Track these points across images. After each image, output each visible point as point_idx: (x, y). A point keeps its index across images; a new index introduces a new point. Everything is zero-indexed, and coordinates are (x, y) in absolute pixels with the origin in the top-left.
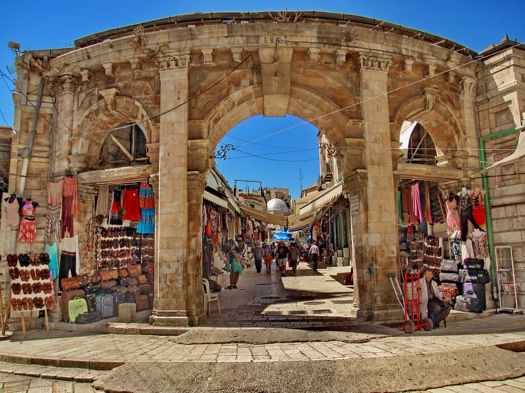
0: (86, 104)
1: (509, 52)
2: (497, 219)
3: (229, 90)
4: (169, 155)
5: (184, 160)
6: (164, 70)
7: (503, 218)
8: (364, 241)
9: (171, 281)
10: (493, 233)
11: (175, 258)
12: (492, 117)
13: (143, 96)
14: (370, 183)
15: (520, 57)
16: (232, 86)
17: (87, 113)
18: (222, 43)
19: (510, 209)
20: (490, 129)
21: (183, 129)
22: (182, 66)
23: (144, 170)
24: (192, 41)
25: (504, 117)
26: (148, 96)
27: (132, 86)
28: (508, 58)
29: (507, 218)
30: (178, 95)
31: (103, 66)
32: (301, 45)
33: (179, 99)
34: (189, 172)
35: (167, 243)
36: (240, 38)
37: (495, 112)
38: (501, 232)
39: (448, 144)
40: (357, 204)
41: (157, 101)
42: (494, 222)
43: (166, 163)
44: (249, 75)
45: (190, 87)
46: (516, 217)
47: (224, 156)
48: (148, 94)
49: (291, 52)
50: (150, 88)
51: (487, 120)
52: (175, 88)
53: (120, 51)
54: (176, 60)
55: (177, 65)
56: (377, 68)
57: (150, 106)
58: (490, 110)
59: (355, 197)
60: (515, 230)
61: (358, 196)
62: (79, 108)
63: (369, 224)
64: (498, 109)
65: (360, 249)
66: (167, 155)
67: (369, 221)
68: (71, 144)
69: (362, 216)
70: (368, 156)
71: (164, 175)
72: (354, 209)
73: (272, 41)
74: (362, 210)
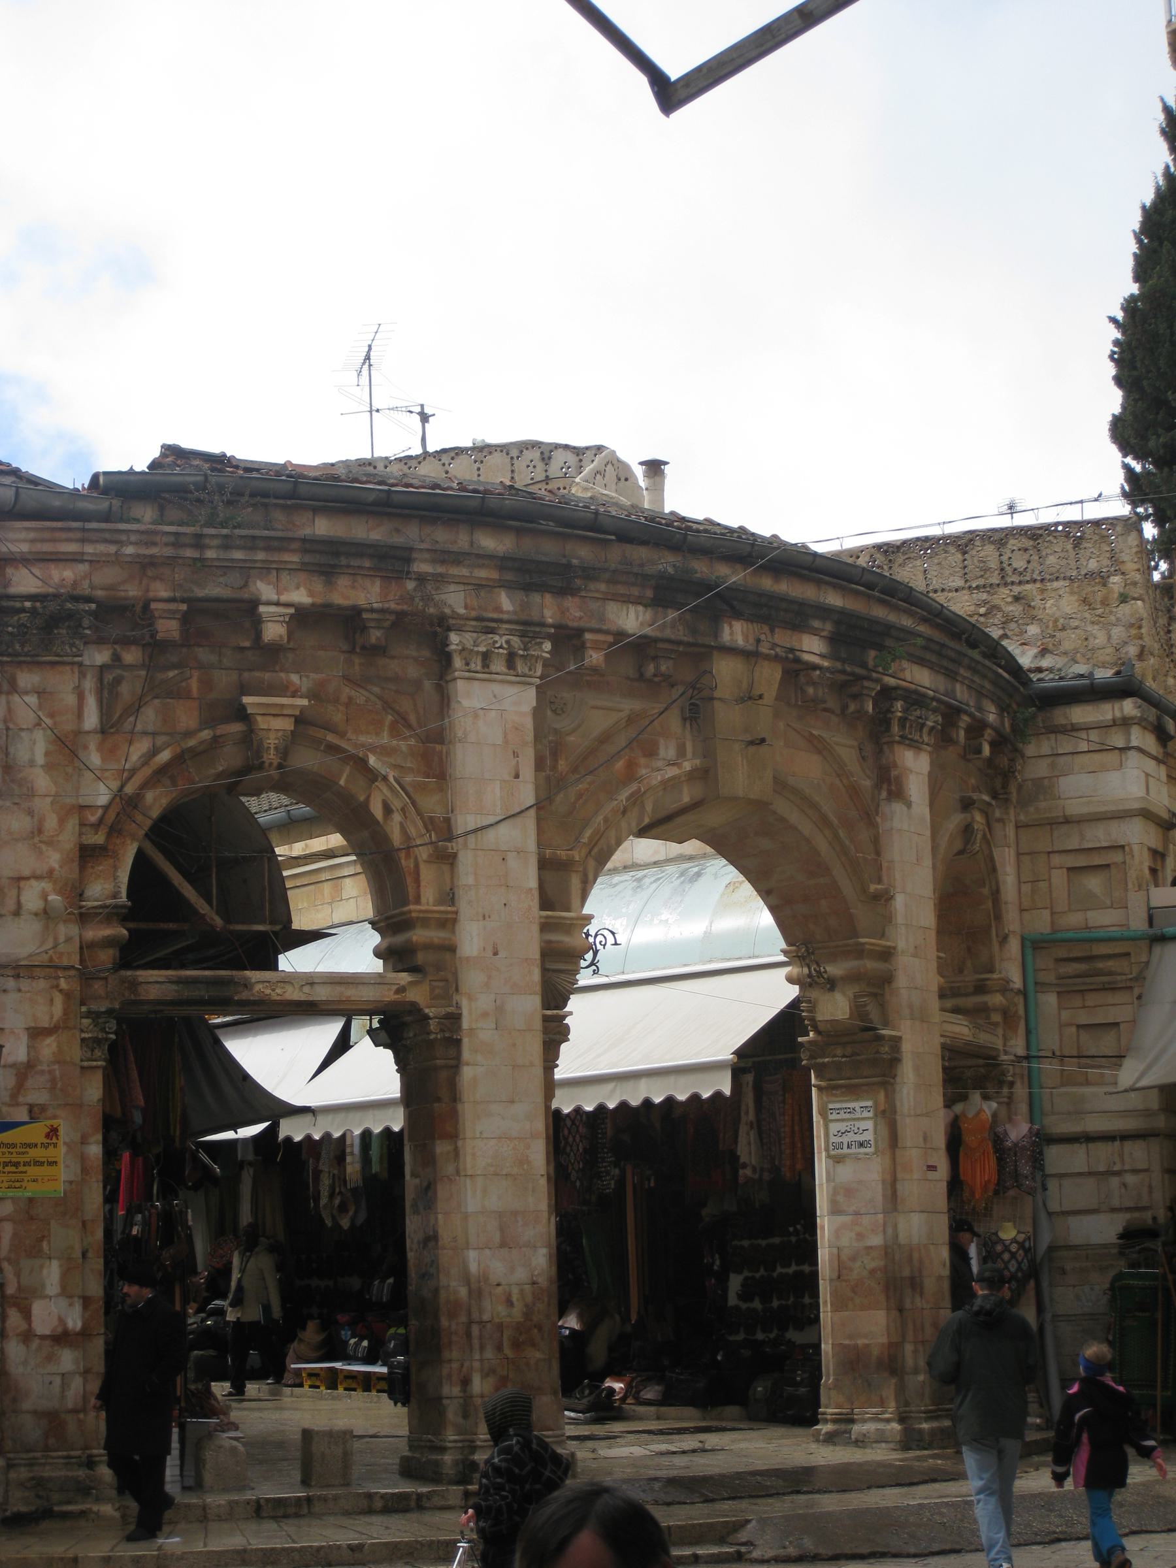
1: (1129, 707)
2: (1062, 1176)
4: (496, 954)
6: (469, 671)
7: (1080, 1174)
9: (516, 1345)
11: (521, 1274)
12: (1059, 878)
13: (385, 739)
14: (907, 1073)
20: (1052, 914)
21: (531, 881)
22: (526, 671)
23: (401, 990)
26: (403, 745)
27: (344, 698)
28: (1125, 723)
29: (1090, 1174)
30: (514, 762)
31: (262, 609)
33: (517, 776)
34: (549, 1012)
35: (502, 1229)
37: (1070, 865)
39: (969, 949)
40: (869, 1125)
43: (489, 977)
45: (537, 738)
46: (1118, 1173)
47: (592, 964)
49: (778, 675)
51: (1043, 885)
52: (506, 742)
53: (328, 573)
57: (409, 779)
58: (1056, 860)
59: (856, 1105)
60: (1113, 1210)
61: (869, 1103)
63: (899, 1186)
64: (1081, 861)
66: (489, 953)
67: (899, 1176)
70: (904, 992)
71: (485, 1015)
72: (845, 1139)
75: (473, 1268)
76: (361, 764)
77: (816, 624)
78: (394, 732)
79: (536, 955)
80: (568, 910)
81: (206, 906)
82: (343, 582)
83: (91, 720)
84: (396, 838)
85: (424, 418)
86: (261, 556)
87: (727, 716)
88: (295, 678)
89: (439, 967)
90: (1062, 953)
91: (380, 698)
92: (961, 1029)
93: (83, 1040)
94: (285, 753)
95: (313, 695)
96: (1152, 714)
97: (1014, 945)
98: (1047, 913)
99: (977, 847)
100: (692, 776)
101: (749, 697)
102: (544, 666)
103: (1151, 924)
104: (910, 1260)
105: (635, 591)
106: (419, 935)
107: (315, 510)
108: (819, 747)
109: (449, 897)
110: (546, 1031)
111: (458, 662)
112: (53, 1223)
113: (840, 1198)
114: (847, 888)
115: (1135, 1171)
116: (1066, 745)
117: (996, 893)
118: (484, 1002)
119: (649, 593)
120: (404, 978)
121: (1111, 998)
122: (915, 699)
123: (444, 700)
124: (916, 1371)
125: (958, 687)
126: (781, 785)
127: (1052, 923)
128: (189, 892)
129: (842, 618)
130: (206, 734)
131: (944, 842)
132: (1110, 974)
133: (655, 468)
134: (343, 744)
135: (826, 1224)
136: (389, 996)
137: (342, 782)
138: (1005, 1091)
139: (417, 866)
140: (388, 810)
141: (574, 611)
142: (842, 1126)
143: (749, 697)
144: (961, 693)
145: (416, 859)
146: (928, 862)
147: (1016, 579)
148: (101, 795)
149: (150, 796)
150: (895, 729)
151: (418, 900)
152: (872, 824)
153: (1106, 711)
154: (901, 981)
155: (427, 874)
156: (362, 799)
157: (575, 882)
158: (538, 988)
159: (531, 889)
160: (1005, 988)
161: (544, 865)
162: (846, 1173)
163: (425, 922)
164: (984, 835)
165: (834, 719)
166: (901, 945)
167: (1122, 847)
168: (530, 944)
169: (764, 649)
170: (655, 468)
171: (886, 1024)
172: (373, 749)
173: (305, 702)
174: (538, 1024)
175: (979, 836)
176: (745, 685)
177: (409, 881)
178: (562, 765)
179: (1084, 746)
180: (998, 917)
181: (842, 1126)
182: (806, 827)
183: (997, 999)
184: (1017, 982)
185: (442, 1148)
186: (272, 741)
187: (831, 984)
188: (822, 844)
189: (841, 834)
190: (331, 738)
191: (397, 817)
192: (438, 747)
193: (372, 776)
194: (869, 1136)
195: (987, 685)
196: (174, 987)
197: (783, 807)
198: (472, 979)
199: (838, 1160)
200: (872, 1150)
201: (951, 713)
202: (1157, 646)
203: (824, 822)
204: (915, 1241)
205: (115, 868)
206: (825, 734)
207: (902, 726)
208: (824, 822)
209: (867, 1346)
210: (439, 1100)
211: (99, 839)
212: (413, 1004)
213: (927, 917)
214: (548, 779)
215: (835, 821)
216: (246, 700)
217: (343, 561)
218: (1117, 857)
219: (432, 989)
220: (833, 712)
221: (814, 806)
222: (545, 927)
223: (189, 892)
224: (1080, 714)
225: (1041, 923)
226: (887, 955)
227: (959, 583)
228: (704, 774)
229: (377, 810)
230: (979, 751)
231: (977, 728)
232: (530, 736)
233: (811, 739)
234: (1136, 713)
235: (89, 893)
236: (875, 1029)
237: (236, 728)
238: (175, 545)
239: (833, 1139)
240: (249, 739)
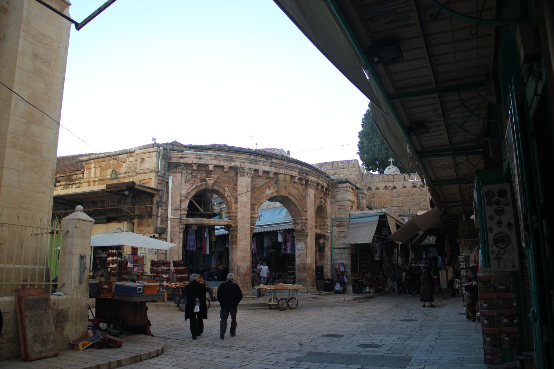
0: (192, 181)
1: (347, 184)
2: (335, 254)
3: (266, 190)
5: (250, 221)
7: (338, 254)
8: (306, 261)
10: (333, 259)
11: (246, 265)
12: (336, 210)
14: (309, 238)
16: (267, 188)
17: (194, 187)
18: (267, 169)
19: (342, 250)
24: (255, 165)
25: (342, 211)
29: (340, 254)
32: (294, 175)
35: (243, 259)
36: (274, 168)
38: (337, 259)
40: (303, 245)
41: (235, 189)
42: (334, 255)
44: (273, 184)
45: (252, 185)
46: (344, 254)
48: (230, 185)
50: (232, 182)
52: (246, 186)
53: (219, 160)
54: (247, 173)
55: (247, 174)
56: (312, 187)
60: (343, 259)
62: (186, 183)
64: (340, 207)
65: (303, 264)
66: (242, 217)
68: (181, 201)
69: (305, 250)
71: (241, 226)
72: (300, 247)
73: (285, 172)
74: (305, 248)
75: (238, 264)
76: (224, 189)
77: (296, 170)
78: (229, 184)
79: (250, 218)
80: (255, 211)
81: (201, 210)
82: (221, 161)
83: (183, 181)
84: (229, 200)
85: (257, 144)
86: (209, 157)
87: (281, 183)
88: (214, 176)
89: (235, 219)
90: (337, 221)
91: (227, 179)
92: (319, 231)
93: (180, 228)
94: (212, 187)
95: (217, 178)
96: (351, 186)
97: (329, 219)
98: (335, 215)
99: (323, 204)
100: (276, 192)
101: (285, 181)
102: (253, 175)
103: (350, 216)
104: (309, 265)
105: (267, 164)
106: (231, 214)
107: (218, 151)
108: (296, 188)
109: (237, 209)
110: (251, 229)
111: (239, 174)
112: (174, 256)
113: (299, 256)
114: (300, 209)
115: (346, 253)
116: (338, 190)
117: (326, 212)
118: (241, 225)
119: (269, 164)
120: (229, 221)
121: (343, 227)
122: (312, 182)
123: (237, 180)
124: (309, 282)
125: (319, 180)
126: (290, 194)
127: (335, 217)
128: (199, 207)
129: (300, 169)
130: (200, 184)
131: (317, 203)
132: (344, 224)
133: (289, 152)
134: (221, 186)
135: (297, 259)
136: (227, 223)
137: (221, 191)
138: (327, 241)
139: (232, 204)
140: (228, 195)
141: (257, 167)
142: (299, 245)
143: (285, 181)
144: (320, 182)
145: (232, 203)
146: (314, 206)
147: (340, 168)
148: (184, 192)
149: (191, 193)
150: (309, 186)
151: (232, 209)
152: (305, 200)
153: (344, 185)
154: (309, 224)
155: (233, 205)
156: (224, 194)
157: (256, 207)
158: (250, 223)
159: (249, 208)
160: (327, 226)
161: (251, 204)
162: (300, 252)
163: (233, 212)
164: (324, 203)
165: (299, 185)
166: (309, 218)
167: (346, 205)
168: (249, 216)
169: (287, 174)
170: (289, 152)
171: (306, 230)
172: (226, 186)
173: (215, 179)
174: (250, 228)
175: (323, 203)
176: (284, 179)
177: (231, 206)
178: (255, 190)
179: (341, 190)
180: (327, 215)
181: (299, 245)
182: (294, 200)
183: (326, 227)
184: (329, 225)
185: (234, 246)
186: (210, 185)
187: (298, 224)
188: (296, 203)
189: (299, 201)
190: (219, 185)
191: (229, 197)
192: (236, 187)
193: (226, 191)
194: (303, 247)
195: (324, 180)
196: (194, 221)
197: (290, 197)
198: (239, 221)
199: (299, 250)
200: (303, 249)
201: (318, 184)
202: (360, 178)
203: (297, 199)
204: (309, 263)
205: (186, 203)
206: (297, 186)
207: (310, 186)
208: (297, 199)
209: (302, 278)
210: (234, 239)
211: (183, 198)
212: (230, 225)
213: (313, 214)
214: (253, 192)
215: (298, 199)
216: (206, 179)
217: (222, 158)
218: (345, 207)
219: (233, 222)
220: (299, 183)
221: (295, 197)
222: (252, 214)
223: (199, 207)
224: (340, 185)
225: (334, 217)
226: (306, 220)
227: (331, 168)
228: (277, 191)
229: (226, 196)
230: (323, 190)
231: (322, 187)
232: (250, 185)
233: (295, 187)
234: (348, 185)
235: (182, 207)
236: (304, 231)
237: (205, 183)
238: (196, 155)
239: (298, 247)
240: (206, 184)
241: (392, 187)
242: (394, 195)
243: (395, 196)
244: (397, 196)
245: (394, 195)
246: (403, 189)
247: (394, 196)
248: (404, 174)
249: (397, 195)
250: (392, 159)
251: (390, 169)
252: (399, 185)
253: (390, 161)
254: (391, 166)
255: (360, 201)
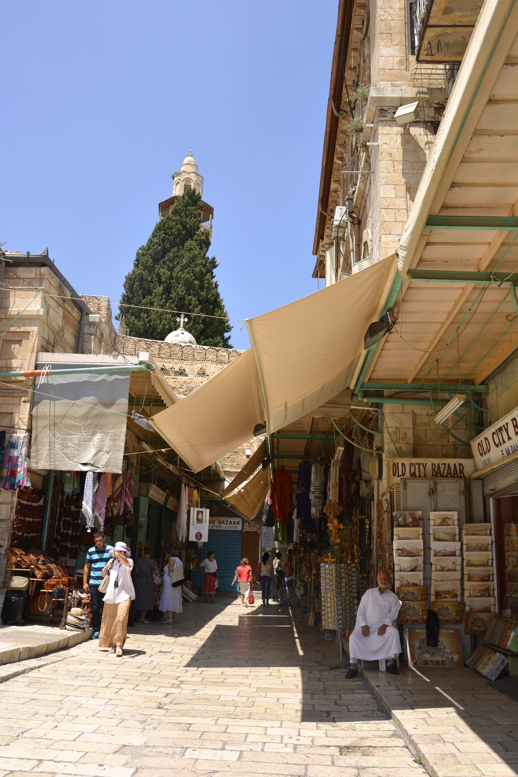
15: (52, 282)
202: (110, 342)
241: (177, 369)
242: (180, 388)
243: (181, 390)
244: (186, 391)
245: (180, 388)
246: (201, 379)
247: (180, 389)
248: (204, 347)
249: (185, 390)
250: (184, 318)
251: (177, 336)
252: (192, 370)
253: (180, 322)
254: (179, 331)
255: (83, 345)
